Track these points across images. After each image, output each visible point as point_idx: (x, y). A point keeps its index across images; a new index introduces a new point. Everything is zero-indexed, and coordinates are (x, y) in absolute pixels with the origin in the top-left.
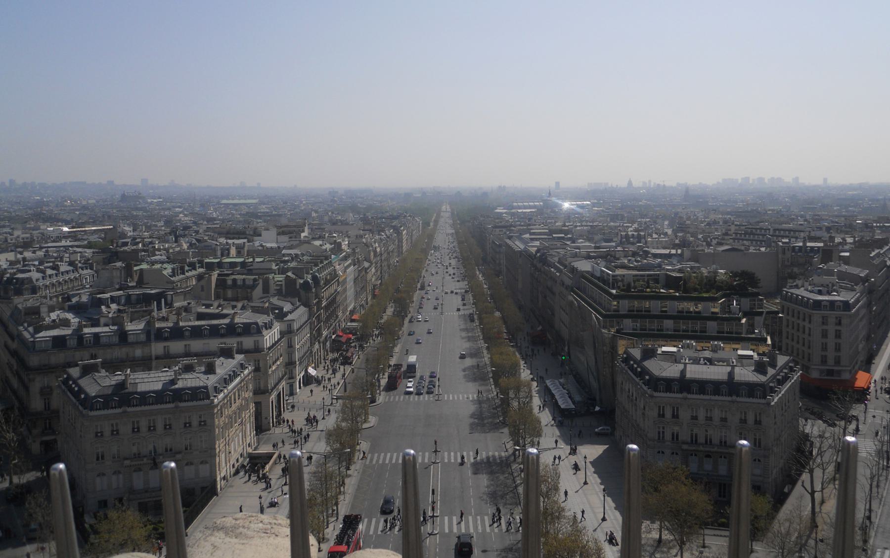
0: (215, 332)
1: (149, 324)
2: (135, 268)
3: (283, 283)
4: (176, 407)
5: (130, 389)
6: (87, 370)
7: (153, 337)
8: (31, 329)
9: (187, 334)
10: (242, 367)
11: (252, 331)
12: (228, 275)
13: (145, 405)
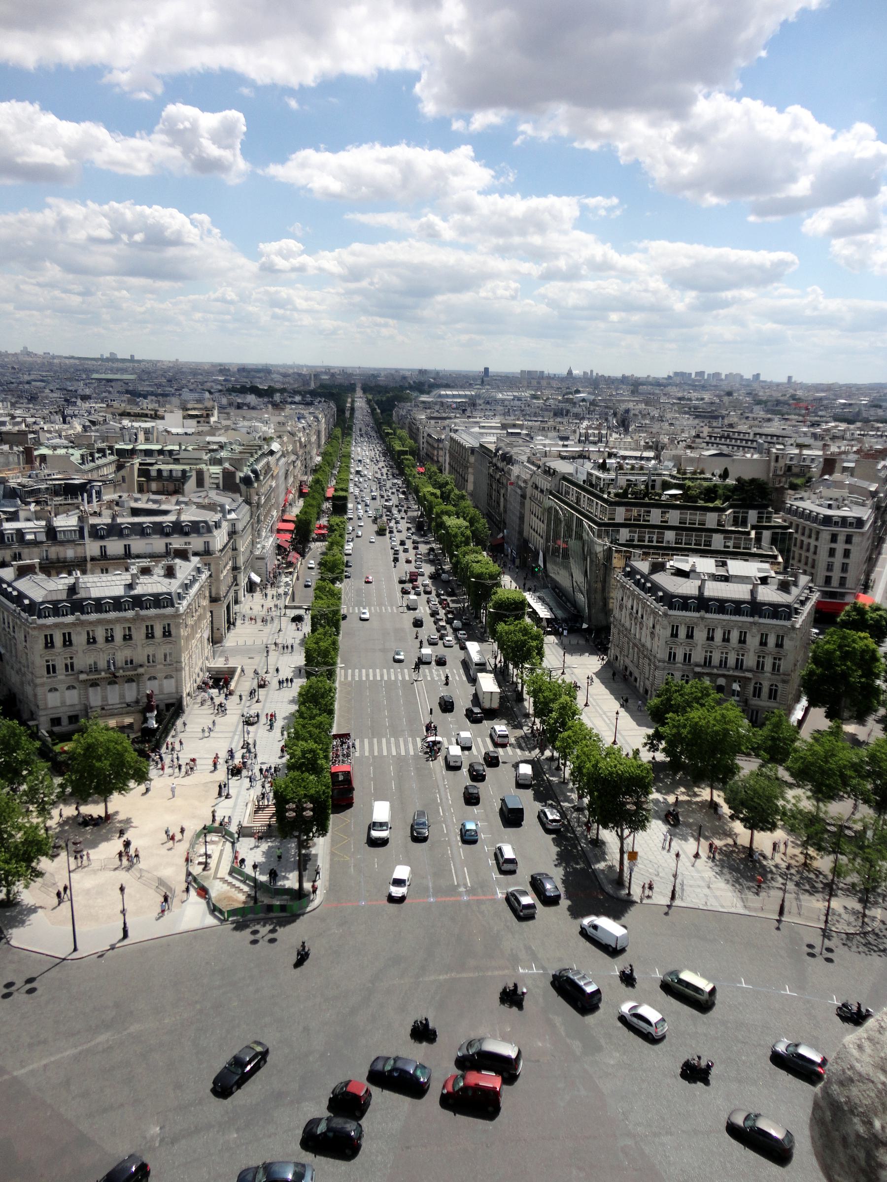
0: (160, 530)
1: (81, 519)
3: (221, 476)
4: (137, 615)
5: (82, 594)
6: (23, 572)
7: (86, 534)
9: (126, 532)
11: (202, 530)
13: (120, 610)
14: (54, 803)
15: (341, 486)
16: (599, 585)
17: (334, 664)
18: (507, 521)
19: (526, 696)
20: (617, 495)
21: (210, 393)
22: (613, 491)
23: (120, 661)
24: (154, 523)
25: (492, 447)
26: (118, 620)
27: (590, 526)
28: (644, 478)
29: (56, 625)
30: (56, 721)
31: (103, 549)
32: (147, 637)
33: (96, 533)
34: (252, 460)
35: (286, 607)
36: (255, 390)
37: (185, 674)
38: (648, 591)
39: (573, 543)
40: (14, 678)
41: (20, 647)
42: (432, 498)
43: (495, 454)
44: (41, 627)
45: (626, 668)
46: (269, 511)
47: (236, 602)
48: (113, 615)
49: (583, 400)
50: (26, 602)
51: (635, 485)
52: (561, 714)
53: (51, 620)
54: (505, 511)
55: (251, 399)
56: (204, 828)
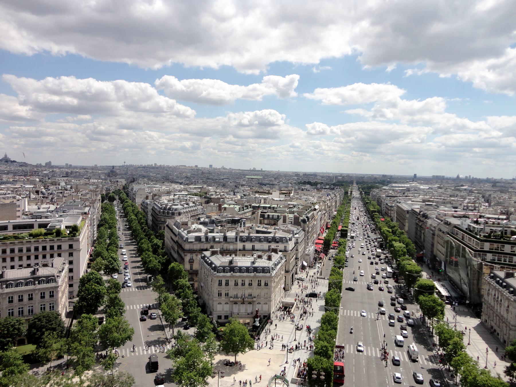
0: (267, 240)
1: (237, 233)
2: (223, 206)
4: (255, 275)
5: (234, 265)
6: (213, 253)
7: (238, 240)
8: (186, 232)
9: (253, 240)
10: (281, 258)
12: (266, 213)
13: (248, 272)
14: (215, 353)
15: (345, 225)
16: (475, 282)
17: (338, 306)
18: (425, 245)
19: (434, 335)
20: (484, 236)
22: (482, 234)
23: (247, 295)
24: (265, 237)
25: (418, 211)
26: (247, 277)
27: (469, 251)
28: (500, 229)
29: (224, 277)
30: (220, 317)
31: (244, 246)
32: (258, 285)
33: (242, 240)
34: (306, 212)
35: (317, 278)
36: (309, 183)
37: (273, 303)
38: (505, 287)
39: (460, 259)
40: (206, 297)
41: (209, 284)
42: (387, 233)
43: (419, 214)
44: (218, 277)
45: (492, 327)
46: (313, 234)
47: (296, 274)
48: (245, 274)
49: (465, 190)
50: (213, 266)
51: (495, 232)
52: (454, 347)
53: (222, 274)
54: (424, 241)
55: (308, 186)
56: (275, 376)
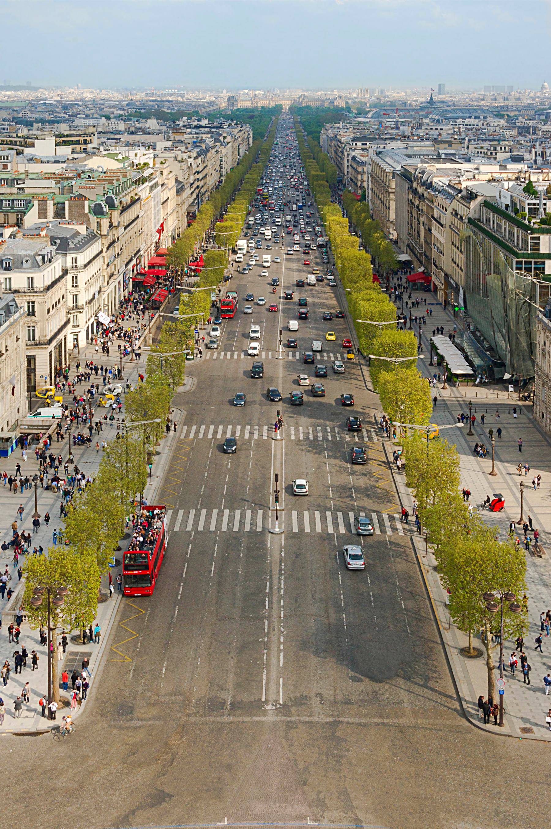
21: (108, 118)
36: (160, 115)
55: (152, 124)
